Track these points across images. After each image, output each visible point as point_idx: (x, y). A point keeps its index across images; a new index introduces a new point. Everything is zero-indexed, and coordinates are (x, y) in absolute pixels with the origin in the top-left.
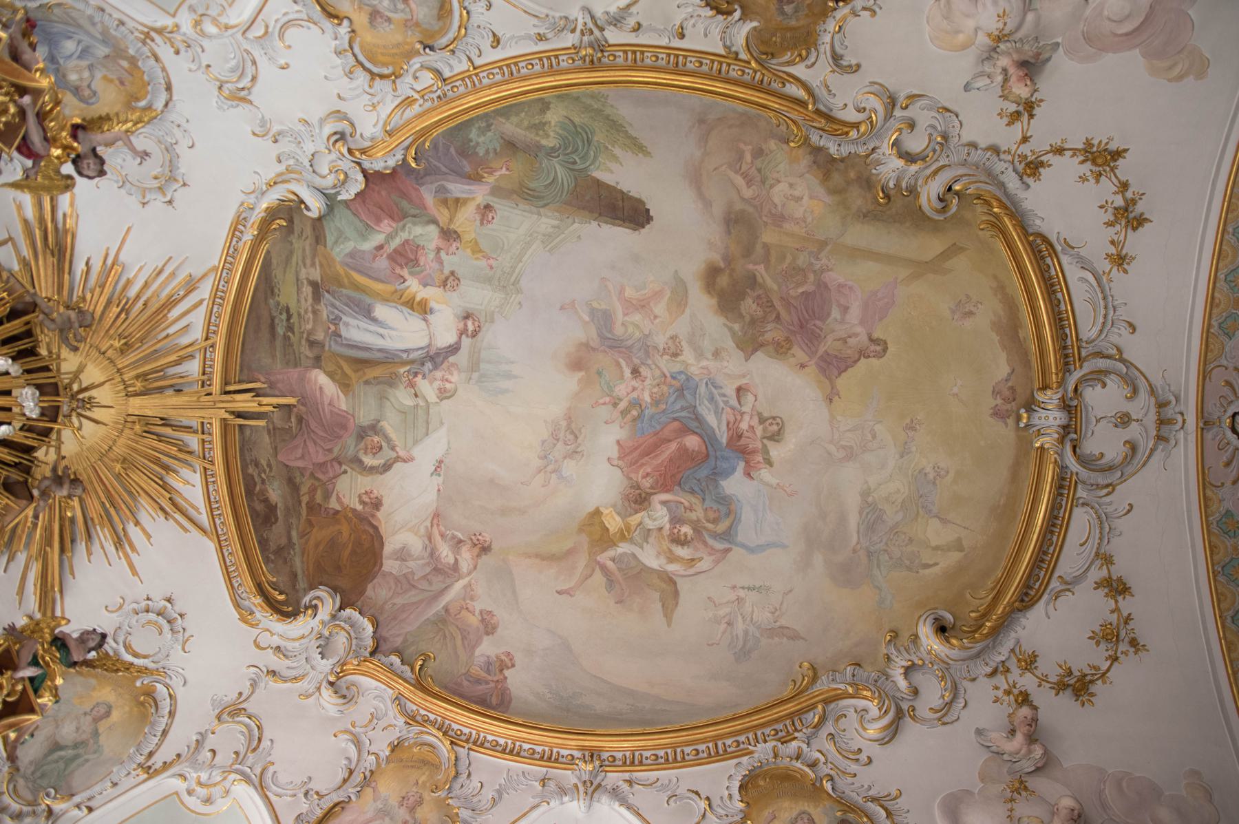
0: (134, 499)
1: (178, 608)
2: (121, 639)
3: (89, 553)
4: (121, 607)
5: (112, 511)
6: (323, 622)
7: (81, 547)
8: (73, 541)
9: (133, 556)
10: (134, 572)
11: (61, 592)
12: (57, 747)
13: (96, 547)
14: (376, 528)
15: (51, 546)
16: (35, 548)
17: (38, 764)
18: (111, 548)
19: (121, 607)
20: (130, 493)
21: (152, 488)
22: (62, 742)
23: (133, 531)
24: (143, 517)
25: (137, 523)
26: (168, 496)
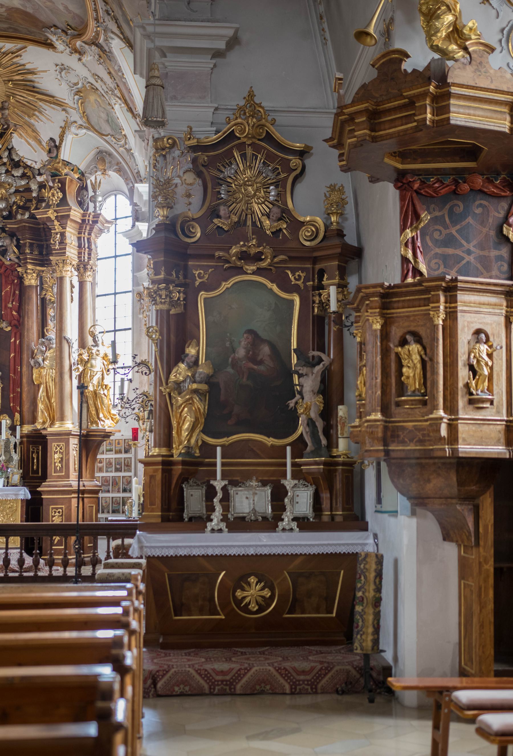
0: (14, 64)
1: (60, 64)
2: (72, 85)
3: (38, 83)
4: (59, 80)
5: (19, 72)
6: (57, 40)
7: (36, 85)
8: (34, 87)
9: (38, 70)
10: (45, 71)
11: (53, 97)
12: (108, 121)
13: (36, 80)
14: (13, 8)
15: (35, 96)
16: (35, 100)
17: (112, 129)
18: (35, 76)
19: (59, 80)
20: (11, 65)
21: (7, 58)
22: (106, 119)
23: (28, 66)
24: (22, 62)
25: (24, 65)
26: (10, 54)
